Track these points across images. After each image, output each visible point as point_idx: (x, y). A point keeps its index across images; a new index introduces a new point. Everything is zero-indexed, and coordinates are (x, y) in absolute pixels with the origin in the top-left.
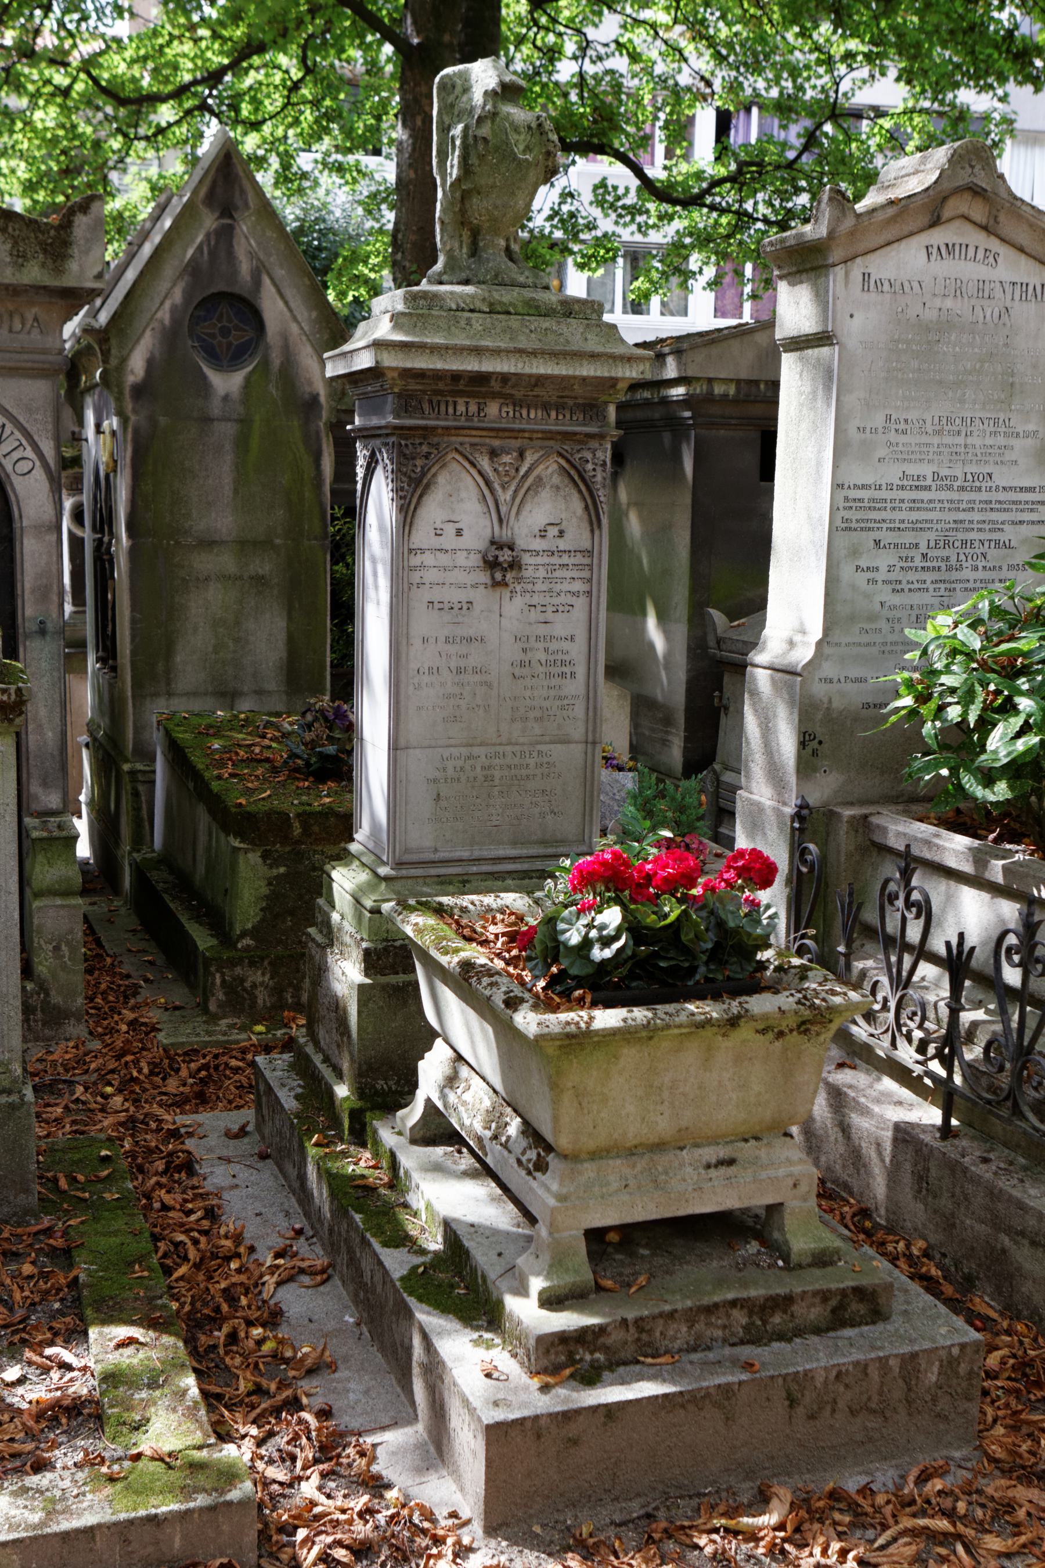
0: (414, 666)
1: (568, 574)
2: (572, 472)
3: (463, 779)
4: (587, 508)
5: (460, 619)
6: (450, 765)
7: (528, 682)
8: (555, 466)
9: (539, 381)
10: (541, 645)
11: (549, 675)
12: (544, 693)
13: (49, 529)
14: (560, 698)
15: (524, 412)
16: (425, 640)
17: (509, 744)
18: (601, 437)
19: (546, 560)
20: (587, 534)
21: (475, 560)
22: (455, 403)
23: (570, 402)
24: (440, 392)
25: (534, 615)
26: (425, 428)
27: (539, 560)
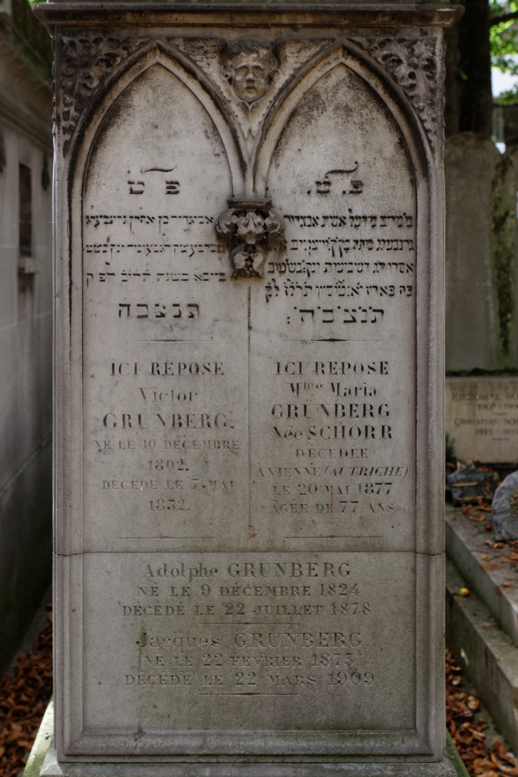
0: (96, 412)
1: (373, 257)
2: (373, 82)
3: (188, 608)
4: (402, 143)
5: (177, 334)
6: (164, 583)
7: (303, 443)
8: (341, 74)
10: (325, 380)
12: (335, 462)
14: (363, 471)
19: (330, 232)
21: (202, 234)
25: (311, 327)
27: (318, 233)
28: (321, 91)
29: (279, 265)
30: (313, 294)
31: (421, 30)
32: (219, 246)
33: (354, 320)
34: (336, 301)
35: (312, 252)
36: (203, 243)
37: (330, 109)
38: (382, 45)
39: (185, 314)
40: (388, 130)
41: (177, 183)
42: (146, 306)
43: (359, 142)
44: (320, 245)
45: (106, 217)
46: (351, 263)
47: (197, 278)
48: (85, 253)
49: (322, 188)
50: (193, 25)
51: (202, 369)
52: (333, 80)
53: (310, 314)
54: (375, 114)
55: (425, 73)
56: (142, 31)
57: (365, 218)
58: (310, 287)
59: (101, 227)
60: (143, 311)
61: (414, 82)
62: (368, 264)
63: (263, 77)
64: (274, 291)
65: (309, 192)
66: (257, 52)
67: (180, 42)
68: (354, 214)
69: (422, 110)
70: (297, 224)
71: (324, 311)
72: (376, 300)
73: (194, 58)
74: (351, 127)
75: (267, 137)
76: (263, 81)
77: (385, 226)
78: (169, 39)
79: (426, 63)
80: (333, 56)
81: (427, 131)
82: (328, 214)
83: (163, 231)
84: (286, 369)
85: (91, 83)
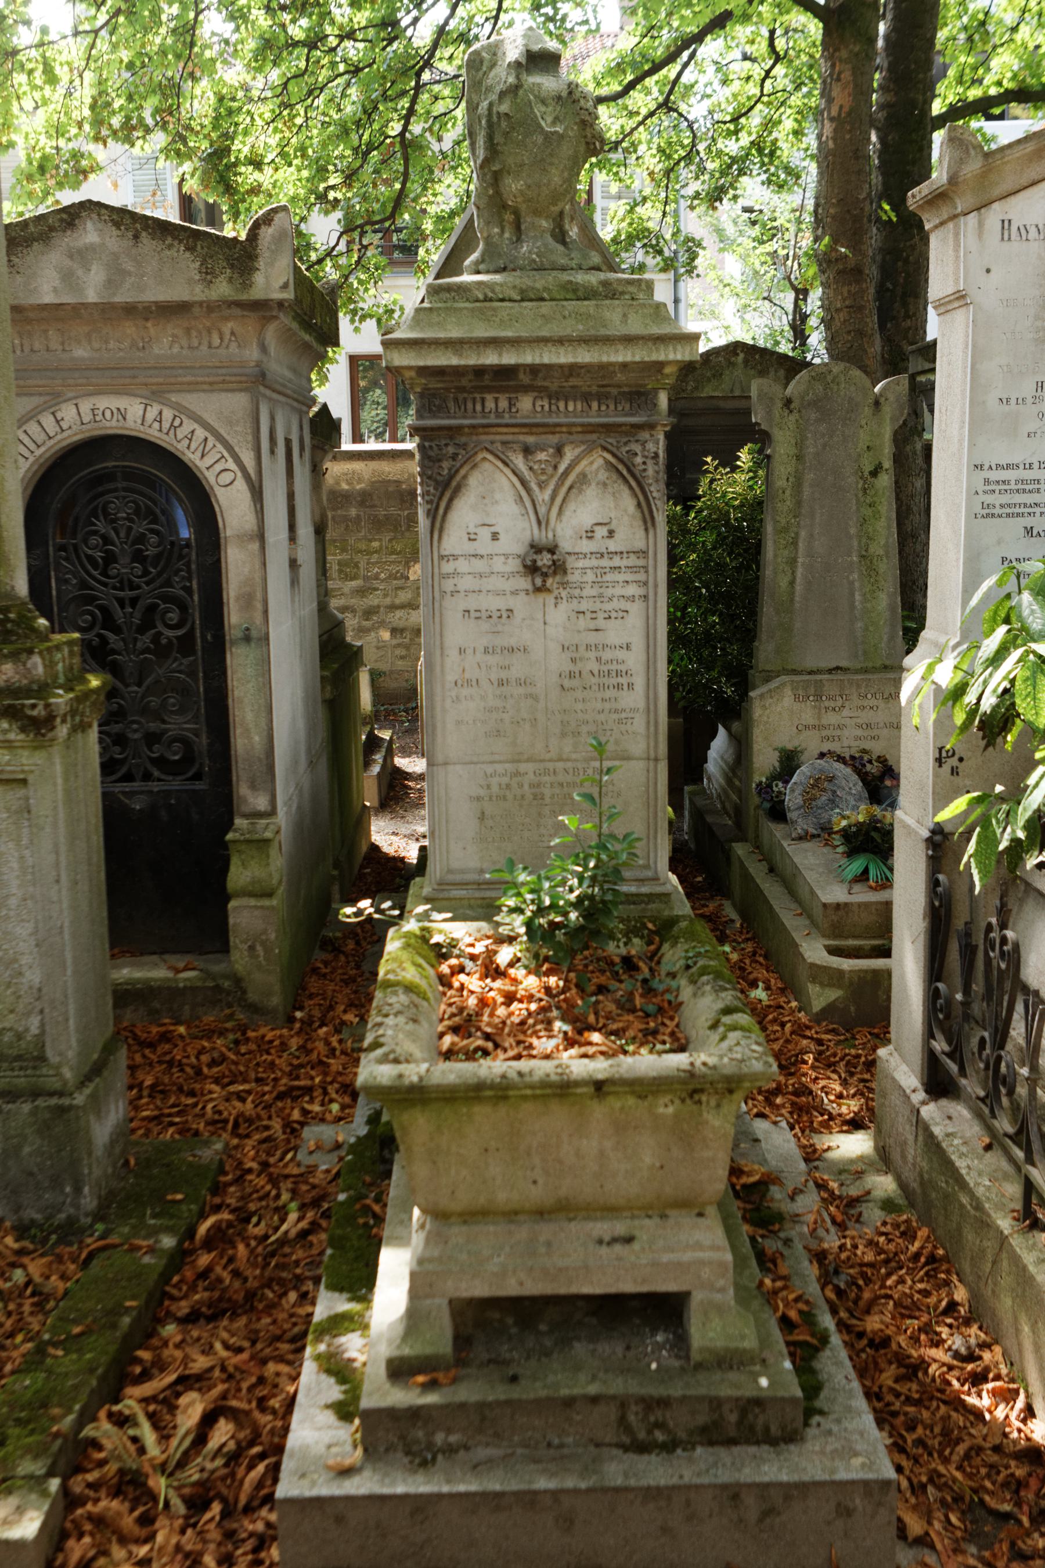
0: (450, 678)
1: (621, 577)
2: (620, 467)
3: (510, 797)
4: (639, 505)
5: (500, 628)
6: (494, 781)
7: (579, 694)
8: (601, 461)
9: (572, 370)
10: (592, 655)
11: (603, 687)
12: (599, 705)
13: (251, 538)
14: (616, 711)
15: (561, 405)
16: (461, 651)
17: (560, 760)
18: (651, 426)
19: (594, 562)
20: (641, 533)
21: (514, 565)
22: (483, 400)
24: (462, 389)
25: (583, 623)
26: (449, 428)
30: (584, 602)
34: (598, 606)
52: (595, 466)
72: (624, 605)
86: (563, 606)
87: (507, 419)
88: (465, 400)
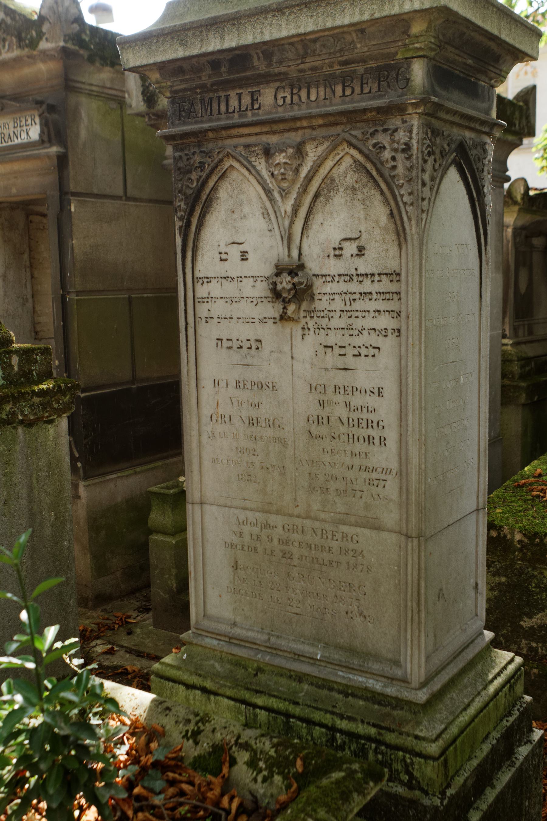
0: (207, 410)
1: (372, 306)
2: (369, 166)
3: (260, 549)
5: (249, 361)
7: (327, 443)
8: (348, 161)
9: (304, 44)
10: (340, 398)
11: (354, 439)
12: (348, 461)
16: (216, 383)
17: (307, 517)
18: (399, 109)
19: (343, 287)
20: (394, 250)
21: (262, 289)
22: (227, 98)
23: (361, 69)
25: (331, 359)
28: (335, 176)
29: (310, 312)
30: (332, 333)
31: (402, 119)
32: (272, 298)
33: (360, 355)
34: (346, 340)
35: (331, 302)
36: (263, 295)
37: (342, 190)
38: (373, 134)
39: (254, 347)
40: (382, 204)
41: (247, 252)
42: (231, 340)
43: (362, 215)
44: (336, 297)
45: (207, 278)
46: (357, 311)
47: (261, 321)
48: (197, 304)
49: (338, 252)
50: (249, 135)
51: (264, 386)
53: (330, 349)
54: (373, 191)
55: (403, 155)
56: (220, 143)
57: (366, 275)
58: (330, 329)
59: (205, 285)
60: (230, 344)
61: (395, 164)
62: (369, 311)
63: (291, 170)
64: (306, 331)
65: (328, 256)
66: (286, 152)
67: (241, 149)
68: (359, 273)
69: (402, 186)
70: (321, 280)
71: (340, 347)
73: (251, 160)
74: (356, 203)
75: (298, 215)
76: (291, 173)
77: (381, 281)
78: (236, 147)
79: (404, 147)
80: (340, 148)
81: (405, 204)
82: (341, 273)
83: (239, 288)
84: (316, 389)
85: (192, 184)
86: (311, 338)
87: (250, 117)
88: (211, 99)
